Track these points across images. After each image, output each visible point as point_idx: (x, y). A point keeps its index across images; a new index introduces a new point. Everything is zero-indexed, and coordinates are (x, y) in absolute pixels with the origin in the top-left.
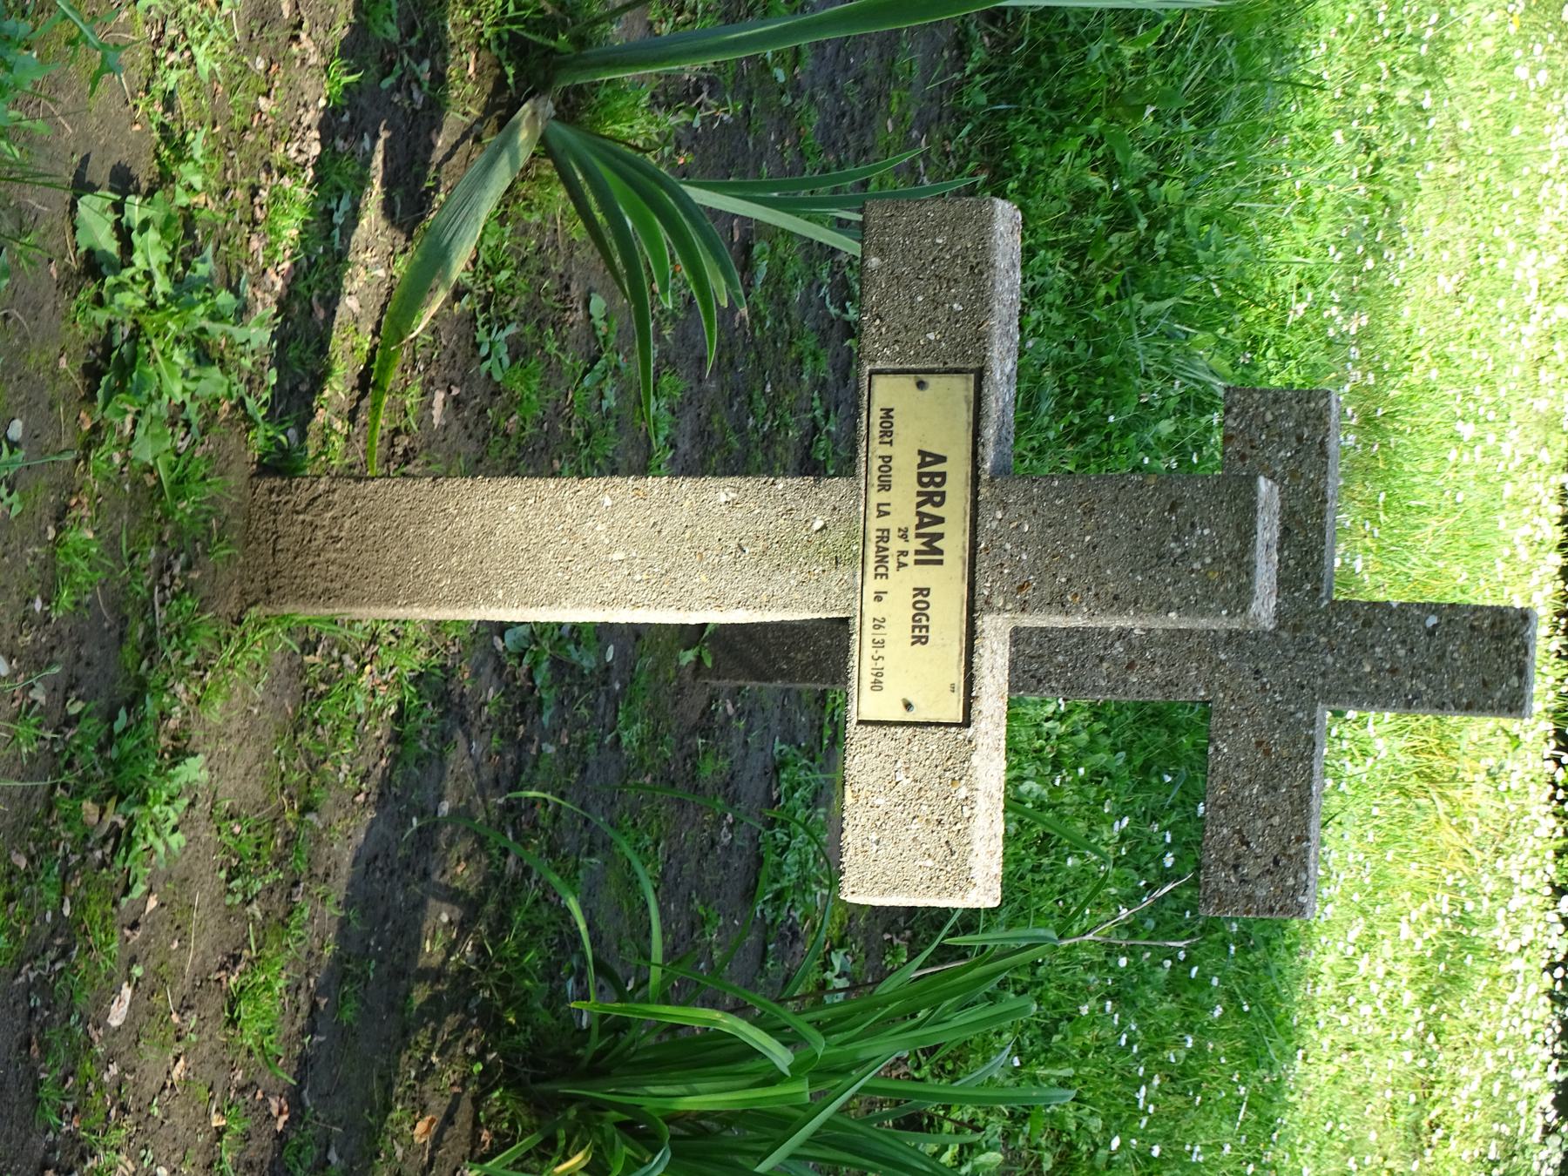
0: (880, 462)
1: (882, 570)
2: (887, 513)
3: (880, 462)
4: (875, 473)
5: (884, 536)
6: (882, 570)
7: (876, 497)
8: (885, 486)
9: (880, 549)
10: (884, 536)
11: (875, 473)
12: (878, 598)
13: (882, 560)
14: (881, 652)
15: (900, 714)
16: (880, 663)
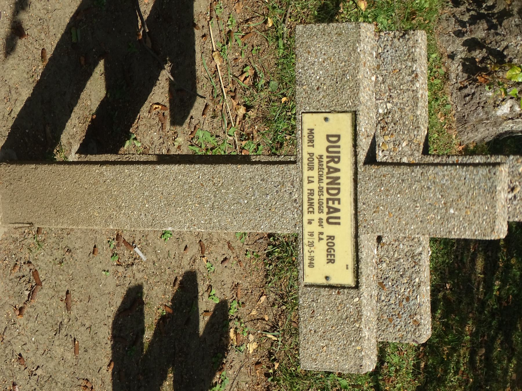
0: (308, 156)
1: (311, 210)
2: (313, 182)
3: (308, 156)
4: (305, 161)
5: (311, 192)
6: (311, 210)
7: (307, 173)
8: (311, 168)
9: (310, 199)
10: (311, 192)
11: (305, 161)
12: (310, 222)
13: (311, 205)
14: (312, 249)
15: (322, 281)
16: (312, 254)
